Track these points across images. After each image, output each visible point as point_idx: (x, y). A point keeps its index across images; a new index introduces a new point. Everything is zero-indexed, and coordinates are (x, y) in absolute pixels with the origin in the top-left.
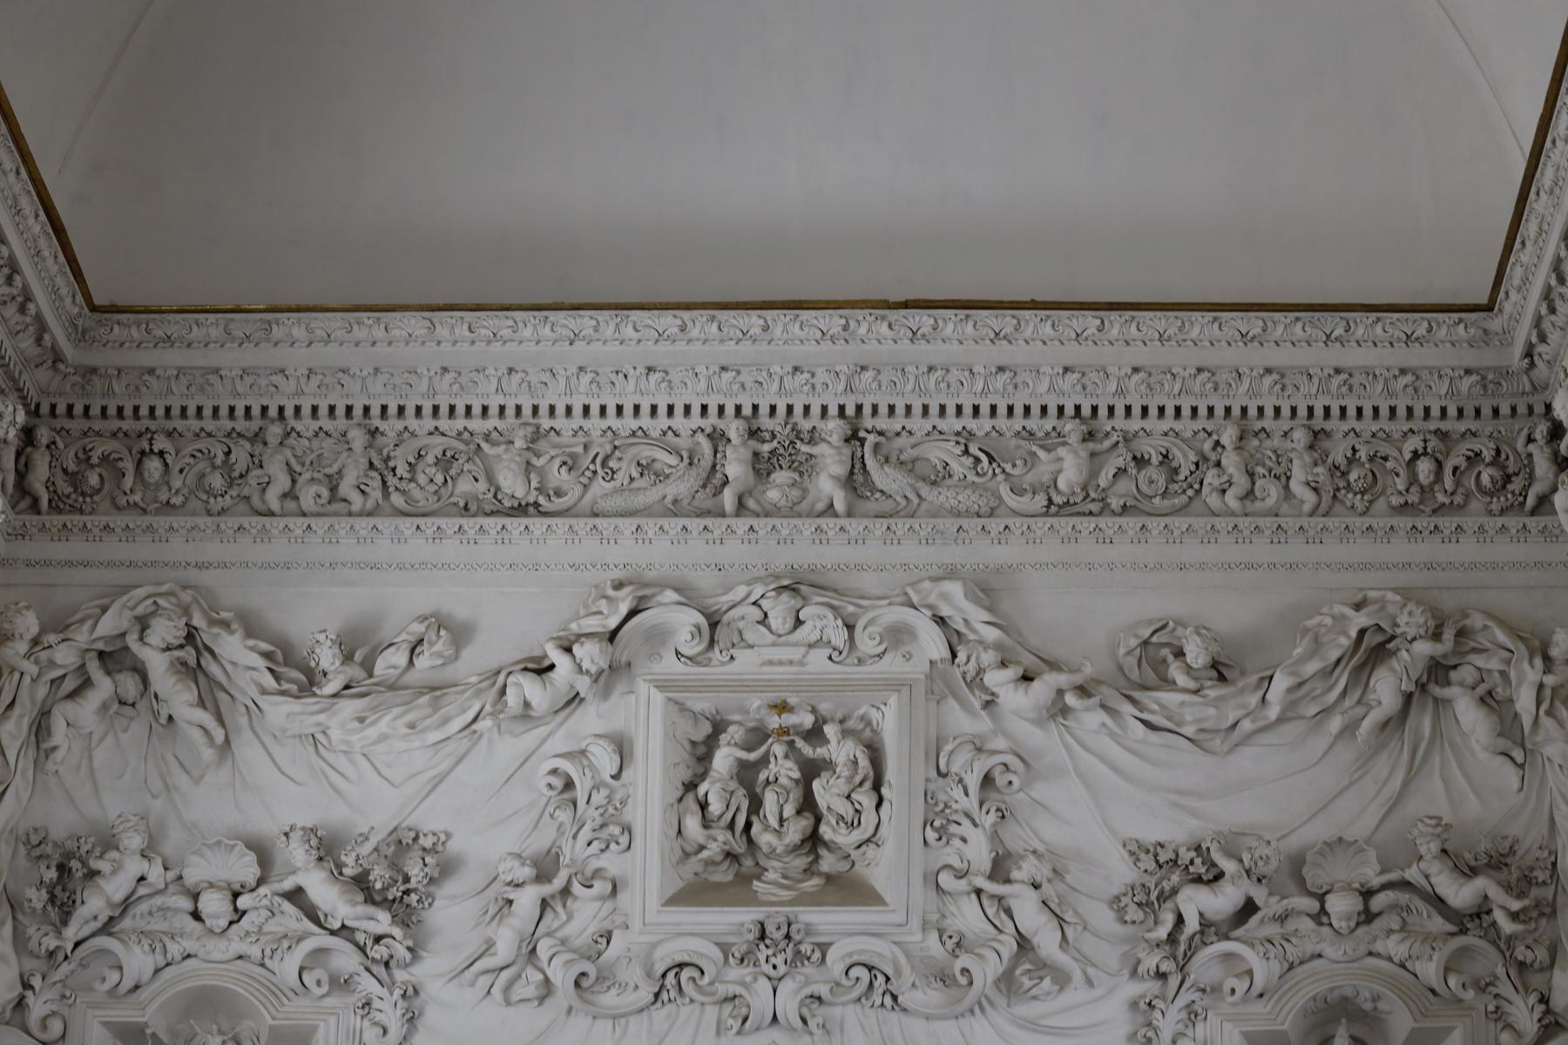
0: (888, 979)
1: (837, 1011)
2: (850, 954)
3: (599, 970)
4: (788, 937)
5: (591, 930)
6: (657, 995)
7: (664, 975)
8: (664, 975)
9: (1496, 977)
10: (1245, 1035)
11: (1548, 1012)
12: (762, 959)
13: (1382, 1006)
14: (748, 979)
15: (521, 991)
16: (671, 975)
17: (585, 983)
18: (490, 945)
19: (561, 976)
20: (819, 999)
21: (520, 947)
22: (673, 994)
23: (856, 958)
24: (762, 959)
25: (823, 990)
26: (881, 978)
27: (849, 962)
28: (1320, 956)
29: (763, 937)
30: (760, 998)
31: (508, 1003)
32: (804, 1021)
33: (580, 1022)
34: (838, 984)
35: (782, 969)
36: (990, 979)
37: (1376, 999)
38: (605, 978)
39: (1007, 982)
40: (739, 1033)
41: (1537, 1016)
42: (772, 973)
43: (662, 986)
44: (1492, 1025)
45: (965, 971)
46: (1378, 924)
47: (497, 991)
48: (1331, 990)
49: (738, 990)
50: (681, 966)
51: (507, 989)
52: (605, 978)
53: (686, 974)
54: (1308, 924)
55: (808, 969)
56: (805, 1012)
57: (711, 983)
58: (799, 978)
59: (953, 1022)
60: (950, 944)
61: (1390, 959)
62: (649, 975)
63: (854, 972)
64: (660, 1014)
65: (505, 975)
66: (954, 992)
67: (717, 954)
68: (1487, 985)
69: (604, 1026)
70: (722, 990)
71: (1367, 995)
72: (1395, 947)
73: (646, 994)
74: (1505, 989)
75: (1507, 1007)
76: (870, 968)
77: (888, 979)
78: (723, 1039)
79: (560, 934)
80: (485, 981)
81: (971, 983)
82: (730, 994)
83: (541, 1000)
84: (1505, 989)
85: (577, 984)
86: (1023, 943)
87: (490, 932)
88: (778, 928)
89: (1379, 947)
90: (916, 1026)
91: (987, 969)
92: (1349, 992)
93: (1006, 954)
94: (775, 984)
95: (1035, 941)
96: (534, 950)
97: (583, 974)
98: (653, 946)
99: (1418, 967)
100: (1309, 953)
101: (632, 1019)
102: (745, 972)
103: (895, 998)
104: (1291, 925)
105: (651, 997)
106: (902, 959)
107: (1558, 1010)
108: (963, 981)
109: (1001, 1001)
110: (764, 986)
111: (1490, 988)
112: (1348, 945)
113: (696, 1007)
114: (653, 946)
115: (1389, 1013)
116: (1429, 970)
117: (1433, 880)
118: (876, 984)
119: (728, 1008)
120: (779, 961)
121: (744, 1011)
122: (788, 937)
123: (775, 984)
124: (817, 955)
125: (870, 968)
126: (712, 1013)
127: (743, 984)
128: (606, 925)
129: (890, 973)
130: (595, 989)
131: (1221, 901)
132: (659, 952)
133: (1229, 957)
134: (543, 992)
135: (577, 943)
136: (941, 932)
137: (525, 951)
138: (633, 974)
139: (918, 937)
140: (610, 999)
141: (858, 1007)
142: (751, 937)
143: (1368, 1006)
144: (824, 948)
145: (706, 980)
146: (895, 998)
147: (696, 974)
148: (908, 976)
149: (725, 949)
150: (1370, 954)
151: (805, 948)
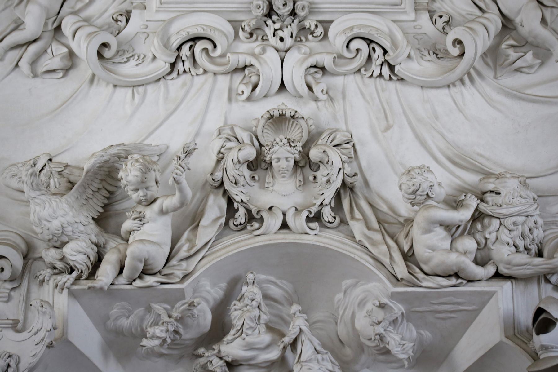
0: (385, 52)
1: (339, 81)
2: (351, 28)
3: (119, 44)
4: (293, 13)
5: (111, 11)
6: (173, 65)
7: (179, 48)
8: (179, 48)
12: (269, 32)
14: (257, 50)
15: (47, 63)
16: (186, 48)
17: (107, 53)
18: (18, 25)
19: (84, 47)
20: (323, 69)
21: (46, 24)
22: (188, 65)
23: (356, 31)
24: (269, 32)
25: (327, 60)
26: (379, 51)
27: (350, 34)
29: (269, 15)
30: (269, 67)
31: (35, 76)
32: (310, 88)
33: (102, 91)
34: (340, 56)
35: (289, 41)
36: (480, 52)
38: (125, 51)
39: (493, 56)
40: (249, 99)
42: (280, 45)
43: (178, 57)
45: (458, 42)
47: (24, 64)
49: (249, 60)
50: (195, 39)
51: (34, 63)
52: (125, 51)
53: (199, 46)
55: (312, 43)
56: (310, 79)
57: (223, 56)
58: (304, 49)
59: (445, 91)
60: (440, 23)
62: (166, 45)
63: (356, 44)
64: (175, 84)
65: (33, 49)
66: (445, 63)
67: (229, 29)
69: (124, 94)
70: (234, 60)
73: (163, 66)
76: (369, 41)
77: (385, 52)
78: (234, 105)
79: (84, 14)
80: (14, 55)
81: (462, 55)
82: (241, 65)
83: (66, 70)
85: (100, 56)
86: (507, 24)
87: (18, 13)
88: (285, 5)
90: (412, 94)
91: (478, 41)
93: (492, 35)
94: (283, 53)
95: (518, 20)
96: (58, 28)
97: (105, 45)
98: (171, 22)
101: (150, 88)
102: (256, 46)
103: (392, 68)
105: (167, 67)
106: (399, 36)
108: (456, 52)
109: (488, 73)
110: (272, 57)
113: (210, 76)
114: (171, 22)
118: (375, 56)
119: (238, 77)
120: (285, 34)
121: (254, 79)
122: (293, 13)
123: (283, 53)
124: (320, 30)
125: (369, 41)
126: (223, 82)
127: (253, 55)
128: (126, 6)
129: (387, 45)
130: (117, 60)
132: (175, 27)
134: (68, 63)
135: (99, 22)
136: (431, 13)
137: (50, 27)
138: (153, 46)
139: (412, 16)
140: (130, 69)
141: (358, 77)
142: (260, 13)
144: (326, 24)
145: (219, 51)
146: (392, 68)
147: (210, 46)
148: (405, 49)
149: (236, 25)
151: (310, 23)
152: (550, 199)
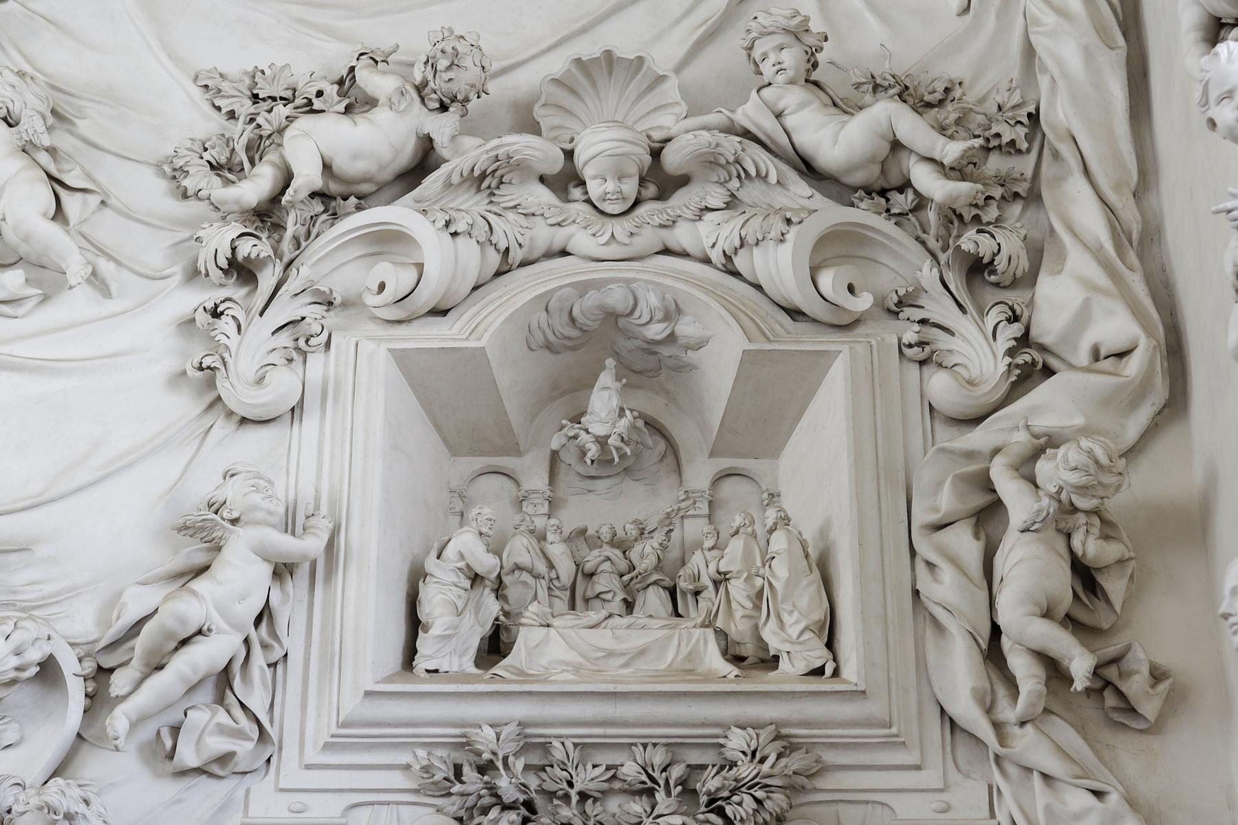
9: (920, 289)
10: (402, 358)
11: (1024, 340)
13: (686, 328)
28: (564, 253)
37: (672, 313)
41: (1004, 343)
44: (915, 368)
46: (683, 200)
48: (583, 288)
54: (542, 196)
61: (707, 261)
68: (900, 304)
71: (654, 300)
72: (714, 234)
74: (940, 308)
75: (942, 341)
84: (940, 308)
89: (682, 236)
92: (617, 298)
99: (757, 263)
100: (541, 248)
104: (508, 195)
107: (1047, 340)
111: (907, 312)
112: (620, 228)
115: (699, 345)
116: (780, 265)
117: (789, 121)
131: (375, 141)
133: (387, 241)
143: (656, 331)
150: (667, 251)
152: (13, 557)
